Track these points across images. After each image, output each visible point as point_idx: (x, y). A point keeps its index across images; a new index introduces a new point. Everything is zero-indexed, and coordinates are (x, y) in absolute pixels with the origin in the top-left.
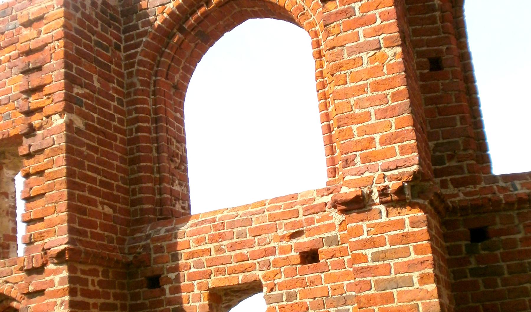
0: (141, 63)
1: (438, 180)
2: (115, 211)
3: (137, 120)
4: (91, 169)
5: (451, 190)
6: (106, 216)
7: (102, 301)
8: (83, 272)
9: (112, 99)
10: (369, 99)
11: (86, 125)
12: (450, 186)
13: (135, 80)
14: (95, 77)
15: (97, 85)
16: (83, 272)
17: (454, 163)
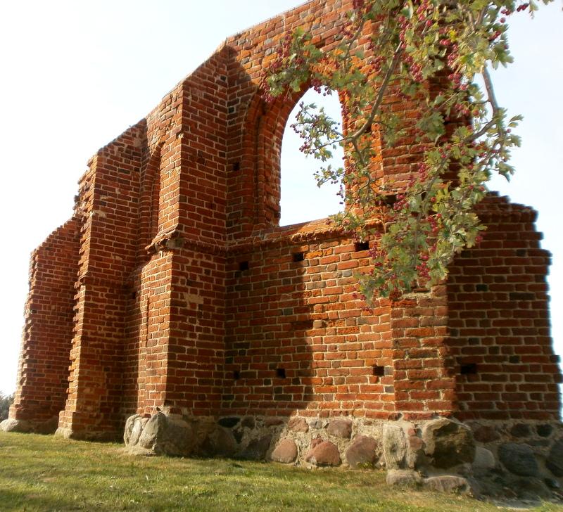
0: (147, 178)
1: (227, 235)
2: (124, 258)
3: (143, 209)
4: (107, 237)
5: (233, 241)
6: (117, 262)
7: (107, 304)
8: (95, 289)
9: (129, 199)
10: (169, 195)
11: (108, 215)
12: (233, 238)
13: (143, 187)
14: (117, 189)
15: (117, 192)
16: (95, 289)
17: (237, 225)
